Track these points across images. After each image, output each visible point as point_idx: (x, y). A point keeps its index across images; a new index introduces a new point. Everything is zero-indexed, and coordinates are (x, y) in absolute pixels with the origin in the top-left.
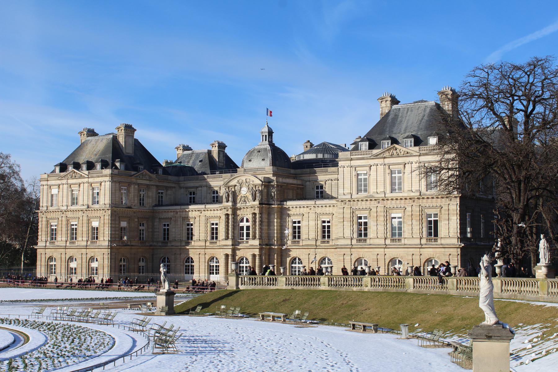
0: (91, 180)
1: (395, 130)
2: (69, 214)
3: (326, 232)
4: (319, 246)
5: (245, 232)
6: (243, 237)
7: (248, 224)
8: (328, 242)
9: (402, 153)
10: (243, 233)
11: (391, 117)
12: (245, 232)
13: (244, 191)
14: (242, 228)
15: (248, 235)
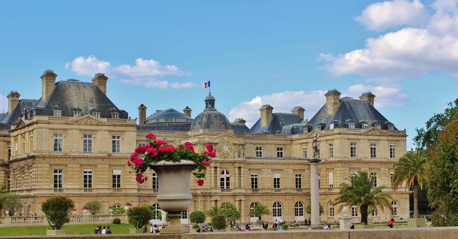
0: (112, 128)
1: (357, 116)
2: (83, 162)
3: (277, 182)
4: (274, 193)
5: (225, 182)
6: (224, 186)
7: (228, 176)
8: (280, 190)
9: (378, 133)
10: (224, 183)
11: (348, 107)
12: (225, 182)
13: (226, 149)
14: (222, 180)
15: (228, 184)
